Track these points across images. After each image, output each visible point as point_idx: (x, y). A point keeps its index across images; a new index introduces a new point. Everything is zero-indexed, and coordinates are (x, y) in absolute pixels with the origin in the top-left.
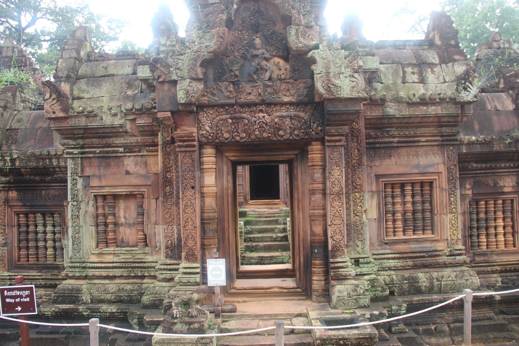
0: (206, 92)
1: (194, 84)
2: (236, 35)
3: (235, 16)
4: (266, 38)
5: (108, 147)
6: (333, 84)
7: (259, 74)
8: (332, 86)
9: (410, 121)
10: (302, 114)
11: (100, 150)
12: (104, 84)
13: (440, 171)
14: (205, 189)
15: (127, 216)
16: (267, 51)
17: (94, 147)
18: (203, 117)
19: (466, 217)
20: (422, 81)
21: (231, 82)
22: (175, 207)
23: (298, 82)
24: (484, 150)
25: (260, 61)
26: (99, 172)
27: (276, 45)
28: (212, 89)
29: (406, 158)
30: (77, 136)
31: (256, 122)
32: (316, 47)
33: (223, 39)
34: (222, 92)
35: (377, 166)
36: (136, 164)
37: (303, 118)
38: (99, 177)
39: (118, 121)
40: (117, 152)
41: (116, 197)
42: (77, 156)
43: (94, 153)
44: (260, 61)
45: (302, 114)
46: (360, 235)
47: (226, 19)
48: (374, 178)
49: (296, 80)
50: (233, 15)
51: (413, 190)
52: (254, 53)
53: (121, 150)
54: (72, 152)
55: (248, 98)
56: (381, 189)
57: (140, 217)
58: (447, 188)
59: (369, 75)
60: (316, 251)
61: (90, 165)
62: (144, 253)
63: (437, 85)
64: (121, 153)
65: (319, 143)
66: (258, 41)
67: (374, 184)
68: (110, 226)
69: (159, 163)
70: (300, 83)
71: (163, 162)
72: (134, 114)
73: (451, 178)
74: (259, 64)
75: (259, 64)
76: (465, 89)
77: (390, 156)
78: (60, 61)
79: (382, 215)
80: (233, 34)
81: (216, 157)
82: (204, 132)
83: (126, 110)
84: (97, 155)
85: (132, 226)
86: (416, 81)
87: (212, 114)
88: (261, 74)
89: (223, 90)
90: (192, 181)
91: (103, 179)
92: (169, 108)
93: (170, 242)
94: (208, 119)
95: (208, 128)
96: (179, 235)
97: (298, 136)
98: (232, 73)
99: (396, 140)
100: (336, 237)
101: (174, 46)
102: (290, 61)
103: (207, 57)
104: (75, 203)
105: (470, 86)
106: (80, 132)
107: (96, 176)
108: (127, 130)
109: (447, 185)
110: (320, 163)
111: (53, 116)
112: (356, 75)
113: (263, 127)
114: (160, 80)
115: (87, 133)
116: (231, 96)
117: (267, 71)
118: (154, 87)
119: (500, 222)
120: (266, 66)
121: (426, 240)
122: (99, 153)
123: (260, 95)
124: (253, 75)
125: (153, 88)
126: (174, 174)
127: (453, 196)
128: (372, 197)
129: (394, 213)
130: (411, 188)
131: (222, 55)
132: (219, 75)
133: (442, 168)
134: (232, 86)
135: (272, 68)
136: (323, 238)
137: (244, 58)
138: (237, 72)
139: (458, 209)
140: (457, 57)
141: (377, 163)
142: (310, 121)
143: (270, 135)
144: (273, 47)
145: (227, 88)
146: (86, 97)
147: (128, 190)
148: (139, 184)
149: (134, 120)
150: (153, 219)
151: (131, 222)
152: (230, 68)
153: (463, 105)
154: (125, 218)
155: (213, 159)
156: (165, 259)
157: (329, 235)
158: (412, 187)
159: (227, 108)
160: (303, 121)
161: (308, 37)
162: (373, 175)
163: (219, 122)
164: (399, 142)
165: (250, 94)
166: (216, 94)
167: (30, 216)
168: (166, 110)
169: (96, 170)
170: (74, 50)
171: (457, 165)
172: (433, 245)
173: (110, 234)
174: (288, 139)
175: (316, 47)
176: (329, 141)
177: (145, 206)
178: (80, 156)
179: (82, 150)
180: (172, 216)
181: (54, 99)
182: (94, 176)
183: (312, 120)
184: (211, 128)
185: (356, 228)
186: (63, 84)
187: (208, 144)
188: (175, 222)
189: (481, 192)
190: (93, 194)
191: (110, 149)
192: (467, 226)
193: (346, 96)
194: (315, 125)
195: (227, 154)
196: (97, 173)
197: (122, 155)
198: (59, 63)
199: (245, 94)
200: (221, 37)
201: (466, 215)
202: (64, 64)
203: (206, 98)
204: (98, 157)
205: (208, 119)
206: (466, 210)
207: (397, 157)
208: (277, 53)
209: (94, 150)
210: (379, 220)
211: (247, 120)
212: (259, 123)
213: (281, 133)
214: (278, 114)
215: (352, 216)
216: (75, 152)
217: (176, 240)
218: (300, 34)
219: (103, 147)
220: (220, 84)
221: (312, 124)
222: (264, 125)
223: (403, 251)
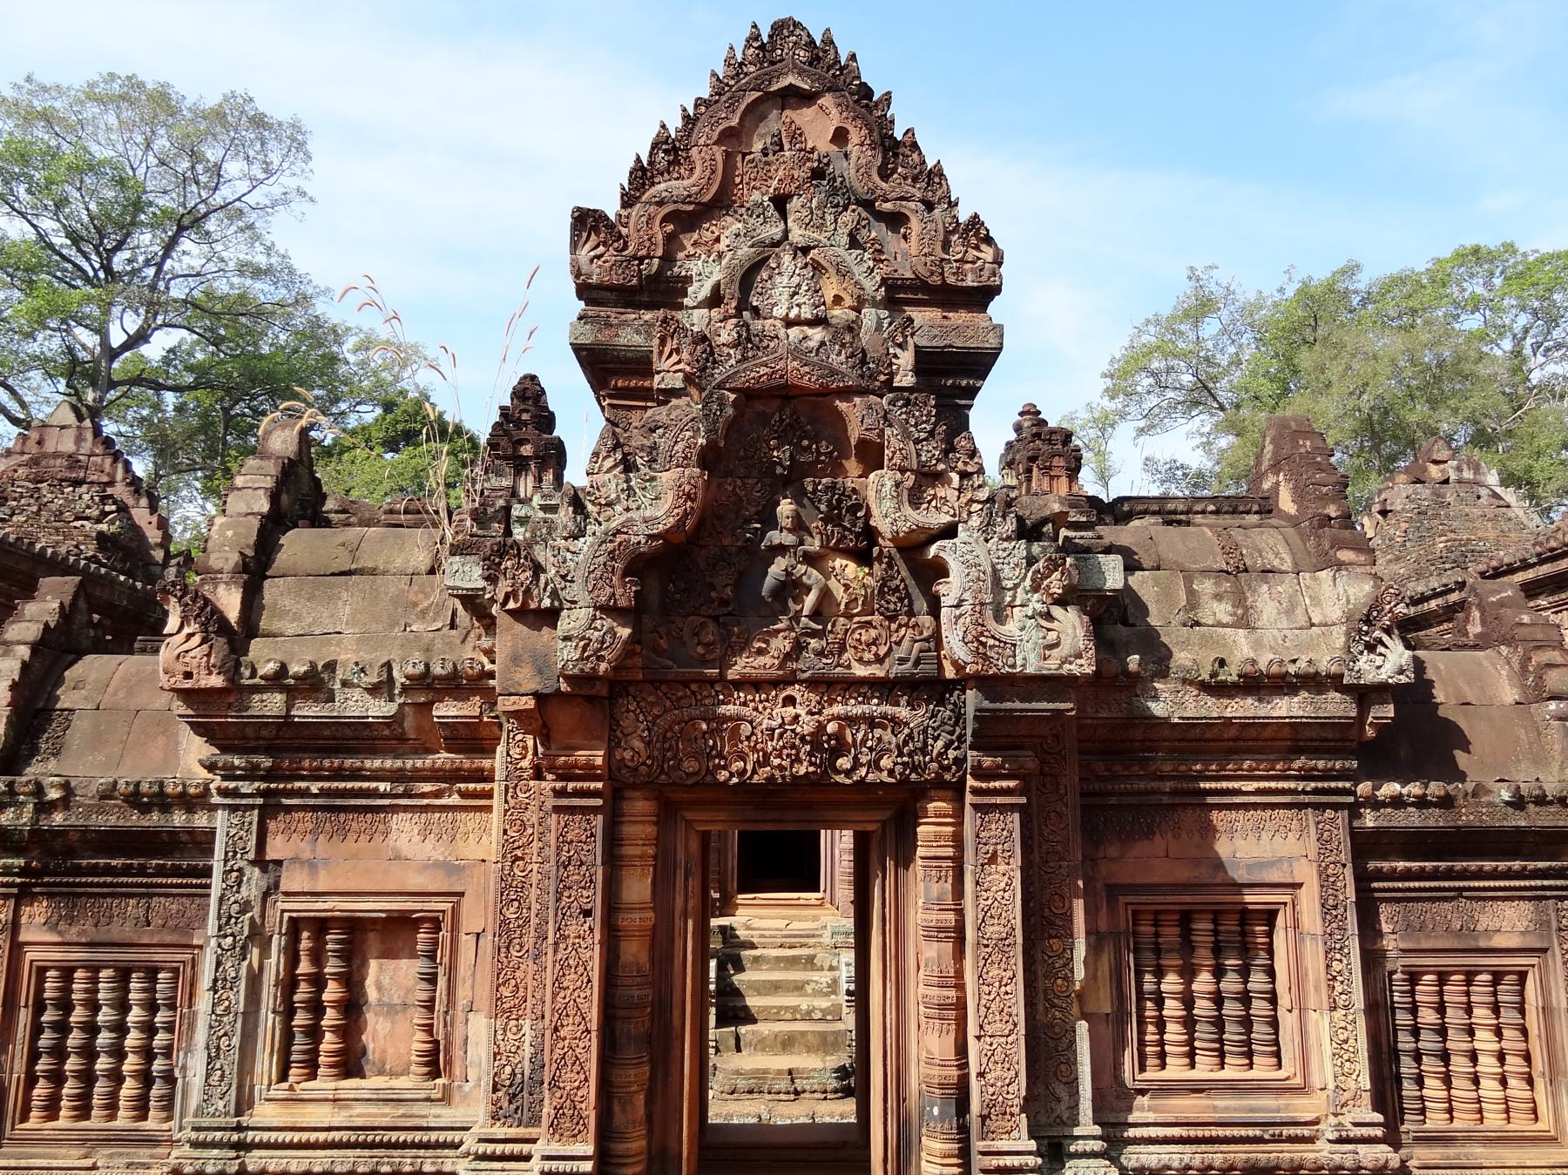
0: (639, 642)
1: (608, 622)
3: (726, 437)
5: (344, 779)
6: (993, 637)
8: (991, 642)
9: (1208, 735)
10: (903, 712)
11: (320, 784)
12: (345, 595)
14: (622, 915)
15: (386, 981)
17: (303, 778)
18: (628, 711)
20: (1244, 621)
21: (709, 617)
22: (530, 963)
24: (1431, 823)
26: (314, 851)
29: (1196, 838)
30: (253, 744)
31: (773, 730)
32: (949, 532)
33: (693, 501)
36: (425, 834)
37: (906, 724)
38: (312, 866)
39: (379, 709)
40: (374, 794)
41: (355, 927)
42: (250, 801)
43: (305, 793)
45: (903, 712)
46: (1063, 1067)
51: (1216, 932)
52: (776, 542)
53: (383, 786)
54: (236, 788)
56: (1123, 925)
57: (424, 985)
58: (1319, 931)
59: (1093, 606)
60: (936, 1111)
61: (288, 831)
62: (428, 1099)
63: (1288, 633)
64: (384, 796)
65: (949, 794)
68: (330, 1013)
69: (494, 832)
71: (505, 832)
72: (429, 687)
73: (1331, 902)
76: (1371, 648)
77: (1149, 833)
78: (219, 520)
80: (719, 486)
81: (656, 823)
82: (628, 755)
83: (407, 677)
84: (312, 802)
85: (397, 1013)
86: (1226, 619)
87: (652, 704)
90: (585, 893)
91: (322, 873)
92: (533, 685)
93: (508, 1069)
94: (641, 718)
95: (637, 744)
96: (538, 1052)
97: (891, 773)
98: (713, 594)
99: (1168, 786)
100: (993, 1074)
101: (553, 509)
104: (229, 940)
105: (1385, 638)
106: (264, 733)
107: (302, 863)
108: (404, 733)
109: (1319, 922)
110: (950, 852)
111: (188, 684)
112: (1057, 611)
113: (793, 746)
114: (511, 605)
115: (287, 740)
116: (708, 657)
117: (810, 590)
118: (493, 618)
121: (1260, 1088)
122: (315, 796)
125: (487, 621)
126: (535, 867)
127: (1338, 956)
129: (1160, 1002)
130: (1211, 926)
134: (711, 626)
136: (954, 1072)
139: (1354, 997)
140: (1345, 555)
141: (1113, 851)
142: (925, 731)
143: (811, 769)
145: (697, 634)
146: (290, 632)
147: (394, 906)
148: (431, 889)
149: (429, 705)
150: (463, 994)
151: (396, 1001)
153: (1365, 695)
154: (379, 988)
155: (650, 830)
156: (490, 1122)
157: (973, 1070)
158: (1215, 922)
159: (694, 687)
160: (906, 731)
161: (929, 502)
162: (1099, 886)
163: (671, 728)
164: (1174, 792)
165: (760, 652)
167: (79, 974)
168: (522, 691)
169: (303, 844)
170: (261, 492)
171: (1349, 865)
172: (1282, 1101)
173: (328, 1036)
174: (863, 779)
175: (949, 532)
176: (976, 792)
177: (443, 955)
178: (260, 801)
179: (264, 786)
180: (521, 993)
181: (190, 636)
182: (295, 860)
183: (930, 731)
184: (648, 744)
185: (1052, 1044)
186: (221, 589)
187: (634, 787)
188: (528, 1011)
189: (1424, 946)
190: (286, 915)
191: (349, 785)
192: (1385, 1049)
193: (1030, 670)
194: (940, 744)
195: (689, 815)
196: (307, 855)
197: (387, 802)
198: (215, 528)
200: (689, 497)
202: (230, 533)
203: (638, 661)
204: (314, 808)
205: (641, 718)
208: (838, 541)
209: (303, 785)
211: (751, 723)
212: (781, 736)
213: (844, 763)
214: (838, 709)
215: (1041, 1008)
216: (243, 791)
217: (526, 1063)
218: (905, 493)
219: (327, 779)
221: (930, 741)
222: (797, 742)
223: (1192, 1116)
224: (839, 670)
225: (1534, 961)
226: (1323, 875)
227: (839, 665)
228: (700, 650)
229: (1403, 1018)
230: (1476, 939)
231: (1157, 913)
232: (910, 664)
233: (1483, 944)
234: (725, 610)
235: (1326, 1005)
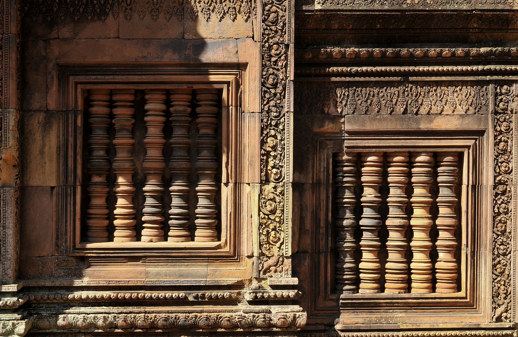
13: (242, 60)
19: (323, 196)
29: (148, 18)
35: (65, 40)
48: (54, 73)
58: (257, 109)
67: (54, 89)
73: (271, 81)
79: (71, 179)
109: (258, 100)
119: (420, 217)
127: (273, 132)
128: (46, 126)
130: (163, 107)
133: (251, 54)
139: (284, 170)
141: (65, 32)
162: (51, 65)
171: (292, 46)
189: (369, 127)
192: (322, 224)
201: (323, 190)
206: (322, 176)
207: (121, 16)
210: (63, 192)
225: (471, 143)
226: (266, 55)
229: (348, 196)
230: (418, 122)
231: (112, 93)
233: (423, 126)
235: (258, 180)
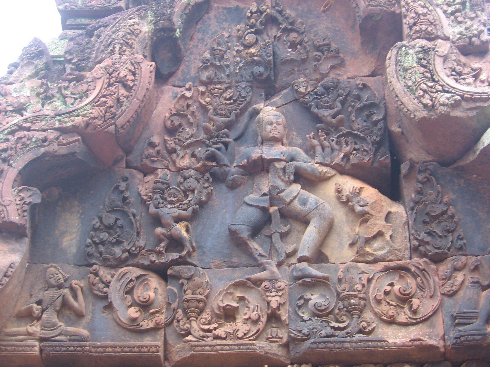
2: (188, 94)
4: (306, 108)
7: (276, 238)
16: (310, 151)
23: (444, 268)
25: (281, 184)
27: (344, 130)
28: (66, 291)
33: (128, 88)
34: (109, 307)
44: (281, 184)
47: (155, 32)
49: (438, 259)
50: (177, 21)
55: (220, 332)
66: (269, 113)
70: (456, 269)
74: (273, 197)
75: (273, 197)
88: (283, 236)
89: (115, 297)
98: (159, 230)
102: (409, 191)
103: (54, 147)
116: (147, 324)
117: (306, 223)
120: (304, 202)
123: (273, 317)
124: (245, 235)
131: (128, 166)
132: (104, 236)
134: (154, 281)
135: (328, 207)
137: (213, 175)
138: (180, 229)
144: (334, 137)
145: (130, 292)
152: (152, 209)
165: (229, 315)
166: (80, 316)
199: (206, 316)
200: (123, 82)
203: (36, 328)
220: (104, 272)
224: (358, 336)
227: (360, 331)
228: (133, 312)
232: (477, 323)
234: (175, 255)
